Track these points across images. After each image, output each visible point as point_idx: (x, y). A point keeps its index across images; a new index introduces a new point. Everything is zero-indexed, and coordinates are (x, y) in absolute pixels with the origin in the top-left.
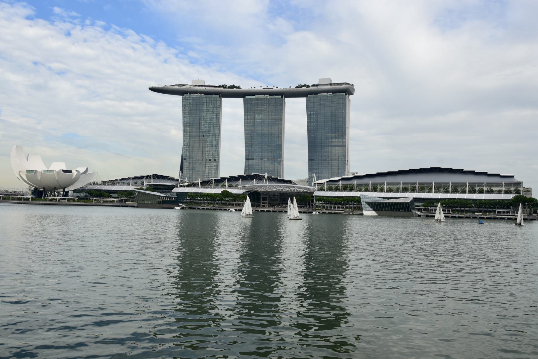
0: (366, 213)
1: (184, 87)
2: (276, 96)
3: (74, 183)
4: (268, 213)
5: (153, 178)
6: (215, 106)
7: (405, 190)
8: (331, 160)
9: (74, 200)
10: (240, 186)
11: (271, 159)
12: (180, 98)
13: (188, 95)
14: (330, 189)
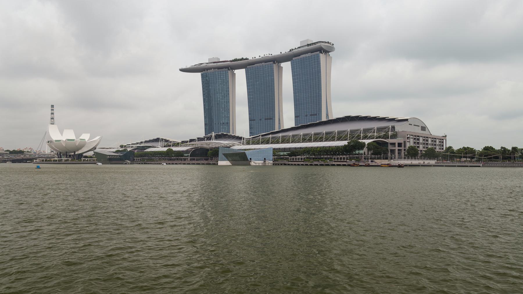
8: (311, 115)
13: (206, 72)
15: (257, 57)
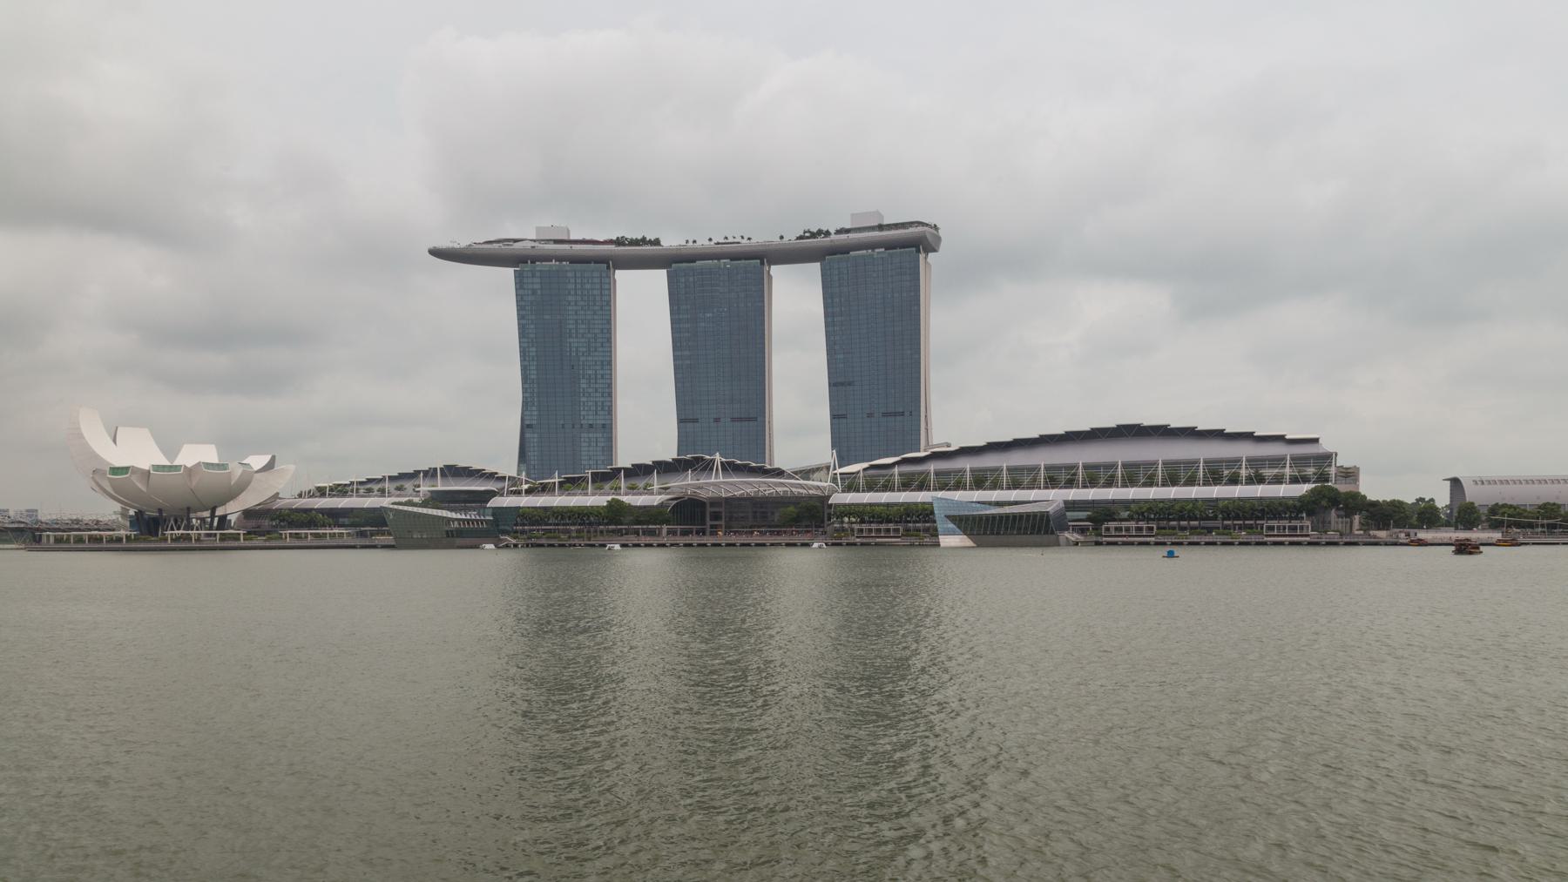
0: (946, 541)
5: (443, 475)
7: (1052, 482)
8: (885, 415)
9: (236, 537)
10: (656, 487)
11: (740, 419)
12: (507, 274)
14: (870, 487)
15: (703, 242)
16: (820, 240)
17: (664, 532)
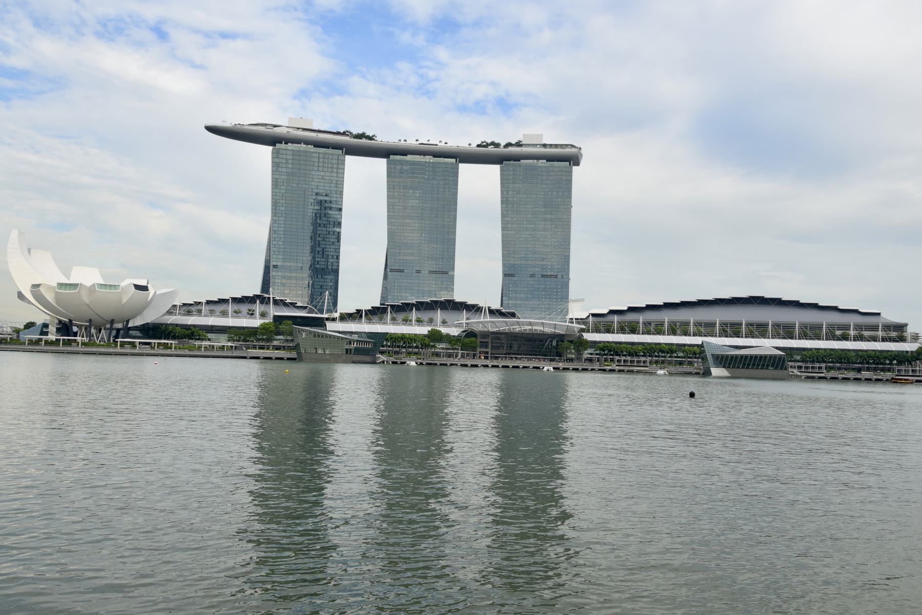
1: (277, 130)
2: (446, 160)
3: (144, 310)
4: (536, 372)
6: (335, 170)
13: (283, 146)
16: (491, 149)
17: (460, 355)
